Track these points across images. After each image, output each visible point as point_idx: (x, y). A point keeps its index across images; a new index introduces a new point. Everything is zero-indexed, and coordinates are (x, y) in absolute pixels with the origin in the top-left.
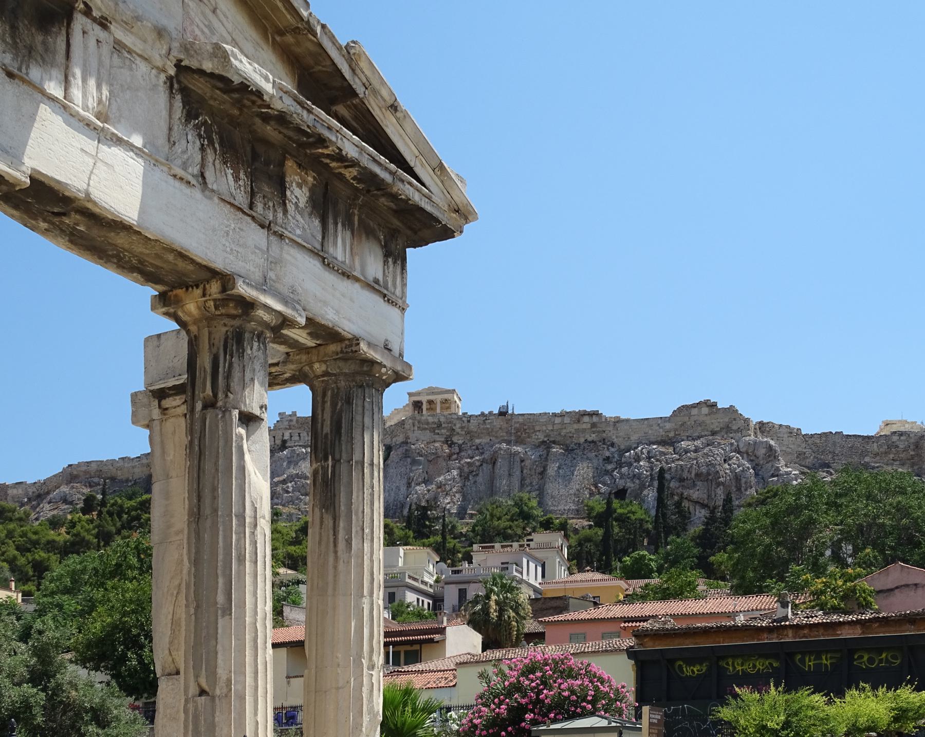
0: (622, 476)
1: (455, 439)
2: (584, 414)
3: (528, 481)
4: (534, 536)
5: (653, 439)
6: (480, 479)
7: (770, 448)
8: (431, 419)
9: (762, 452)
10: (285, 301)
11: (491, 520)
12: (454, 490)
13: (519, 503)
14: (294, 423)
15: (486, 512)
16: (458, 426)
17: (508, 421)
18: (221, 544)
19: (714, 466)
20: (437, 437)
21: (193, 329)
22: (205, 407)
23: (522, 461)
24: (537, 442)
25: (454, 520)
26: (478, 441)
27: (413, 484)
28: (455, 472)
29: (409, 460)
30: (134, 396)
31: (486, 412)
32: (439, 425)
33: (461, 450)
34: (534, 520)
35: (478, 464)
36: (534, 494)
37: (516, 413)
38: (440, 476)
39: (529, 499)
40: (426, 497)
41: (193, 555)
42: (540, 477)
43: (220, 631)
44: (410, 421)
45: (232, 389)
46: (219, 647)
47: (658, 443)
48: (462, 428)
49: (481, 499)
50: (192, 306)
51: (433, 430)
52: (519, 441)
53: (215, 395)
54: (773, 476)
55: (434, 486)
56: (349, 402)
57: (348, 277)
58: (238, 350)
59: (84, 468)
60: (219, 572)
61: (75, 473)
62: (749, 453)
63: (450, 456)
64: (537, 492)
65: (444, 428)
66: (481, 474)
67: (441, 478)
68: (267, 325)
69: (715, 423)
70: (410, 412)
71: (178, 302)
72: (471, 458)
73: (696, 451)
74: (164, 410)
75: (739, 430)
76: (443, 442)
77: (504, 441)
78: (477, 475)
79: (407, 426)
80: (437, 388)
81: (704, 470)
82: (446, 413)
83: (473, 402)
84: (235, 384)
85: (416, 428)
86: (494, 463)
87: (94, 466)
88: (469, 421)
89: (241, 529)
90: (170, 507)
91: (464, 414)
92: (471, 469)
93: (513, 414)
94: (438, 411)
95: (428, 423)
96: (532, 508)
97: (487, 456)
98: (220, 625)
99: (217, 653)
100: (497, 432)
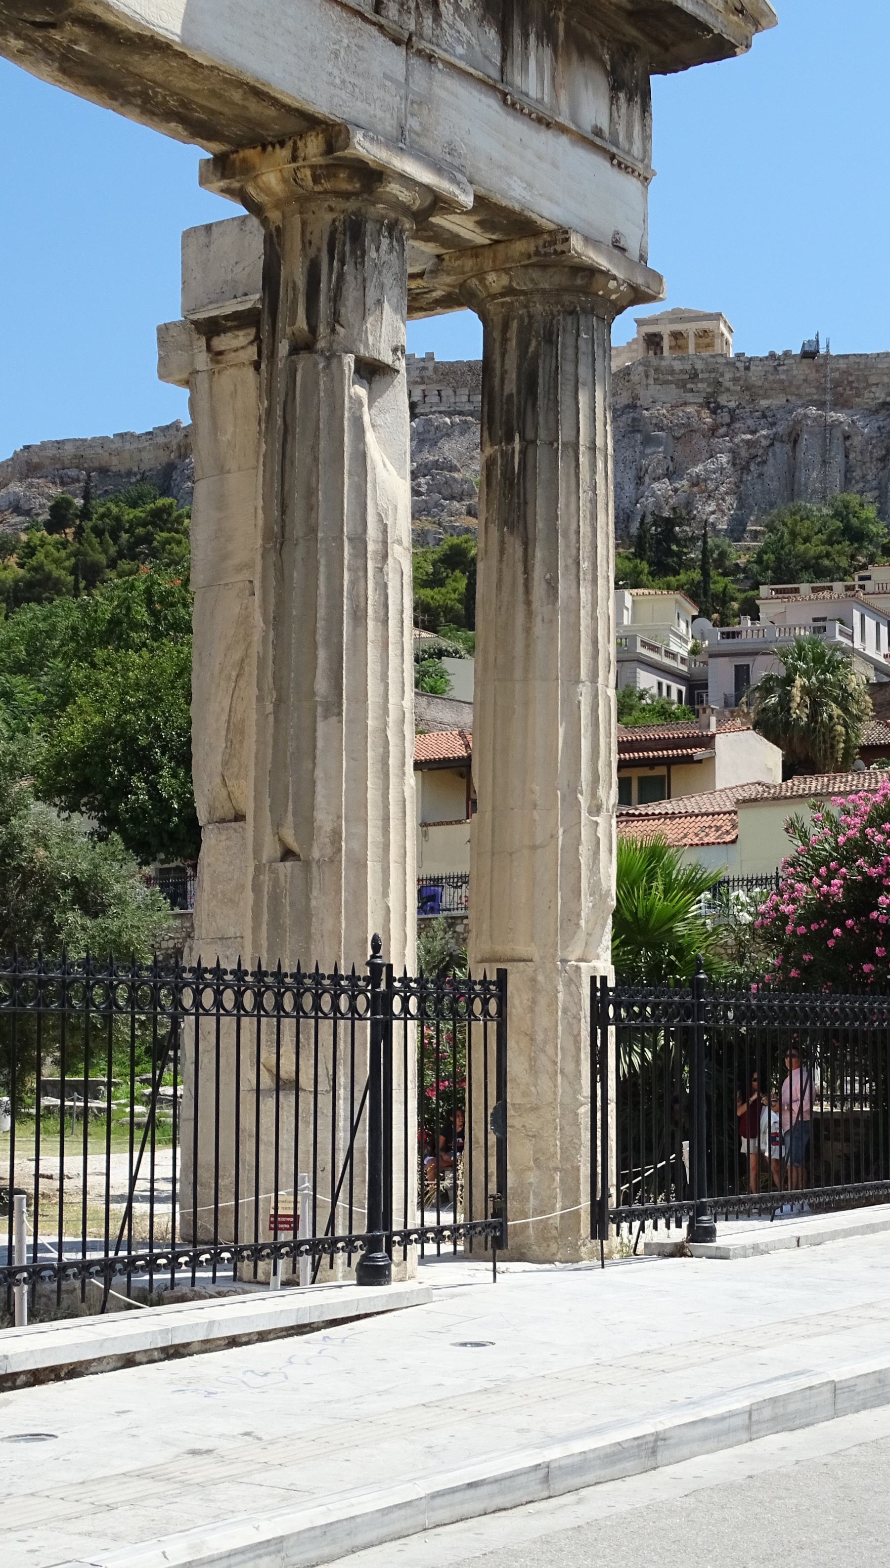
1: (723, 400)
3: (857, 474)
4: (872, 570)
6: (769, 470)
8: (677, 366)
10: (437, 168)
11: (793, 542)
12: (723, 489)
13: (843, 513)
14: (430, 372)
15: (782, 528)
16: (728, 376)
17: (818, 368)
18: (322, 589)
20: (690, 397)
21: (274, 216)
22: (295, 350)
23: (847, 438)
24: (873, 404)
25: (725, 542)
26: (764, 403)
27: (647, 480)
28: (724, 459)
29: (639, 436)
30: (163, 331)
31: (779, 353)
32: (694, 376)
33: (733, 419)
34: (871, 542)
35: (765, 443)
36: (869, 496)
37: (833, 353)
38: (695, 465)
39: (862, 505)
40: (671, 502)
41: (272, 608)
42: (880, 465)
43: (320, 744)
44: (641, 368)
45: (342, 320)
46: (319, 773)
48: (735, 380)
49: (772, 505)
50: (272, 176)
52: (840, 403)
53: (313, 329)
55: (685, 482)
56: (550, 338)
57: (548, 125)
58: (353, 252)
60: (320, 639)
63: (713, 430)
64: (876, 493)
65: (702, 381)
66: (771, 461)
67: (698, 469)
68: (405, 209)
70: (640, 352)
71: (247, 170)
72: (753, 433)
74: (216, 355)
76: (701, 405)
77: (813, 403)
78: (764, 462)
79: (635, 378)
80: (690, 311)
82: (705, 354)
83: (756, 332)
84: (348, 311)
85: (651, 381)
86: (795, 441)
88: (747, 368)
89: (360, 562)
90: (226, 522)
91: (738, 355)
92: (752, 451)
93: (827, 356)
94: (691, 350)
95: (672, 372)
96: (867, 520)
98: (319, 733)
99: (314, 783)
100: (798, 388)
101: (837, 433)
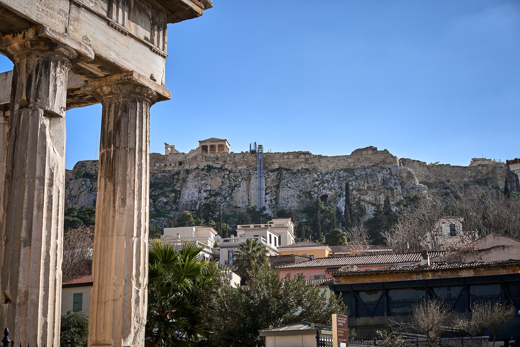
18: (26, 197)
22: (21, 107)
41: (6, 204)
43: (22, 257)
45: (40, 96)
46: (21, 268)
53: (28, 100)
58: (45, 72)
60: (24, 216)
89: (41, 187)
98: (22, 253)
99: (18, 272)
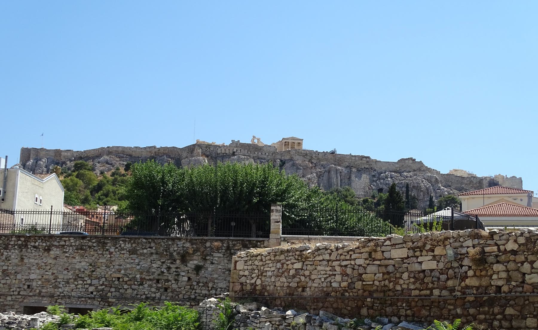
0: (381, 183)
1: (313, 161)
2: (363, 157)
3: (343, 181)
5: (391, 170)
6: (324, 178)
7: (436, 179)
9: (433, 180)
17: (334, 156)
19: (419, 184)
26: (322, 163)
28: (315, 175)
47: (394, 172)
51: (304, 156)
52: (339, 165)
54: (438, 189)
59: (115, 149)
61: (111, 151)
62: (429, 180)
63: (312, 168)
67: (309, 176)
69: (415, 167)
73: (410, 177)
75: (424, 171)
81: (416, 185)
87: (120, 149)
97: (327, 169)
101: (338, 172)
